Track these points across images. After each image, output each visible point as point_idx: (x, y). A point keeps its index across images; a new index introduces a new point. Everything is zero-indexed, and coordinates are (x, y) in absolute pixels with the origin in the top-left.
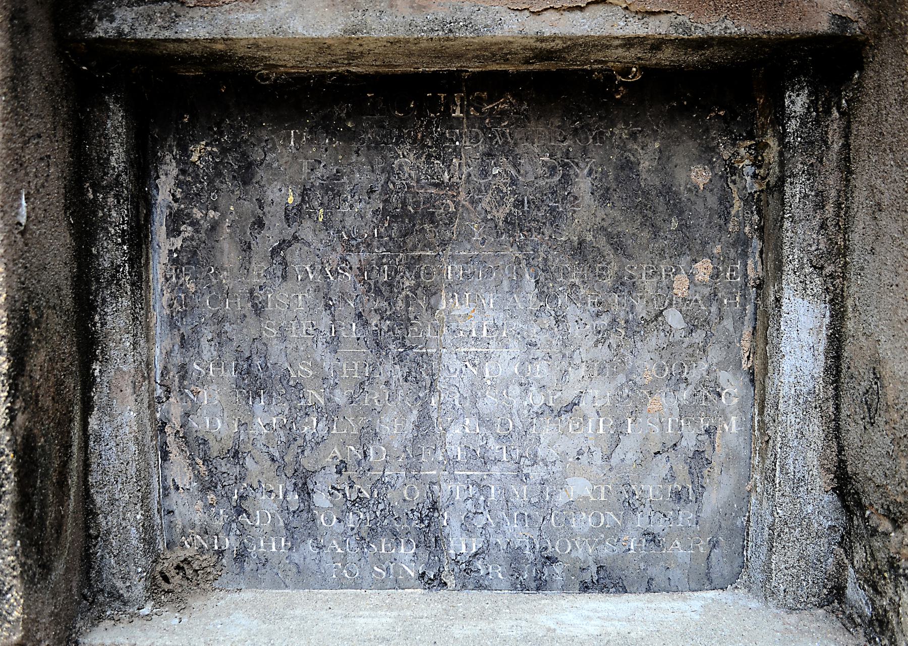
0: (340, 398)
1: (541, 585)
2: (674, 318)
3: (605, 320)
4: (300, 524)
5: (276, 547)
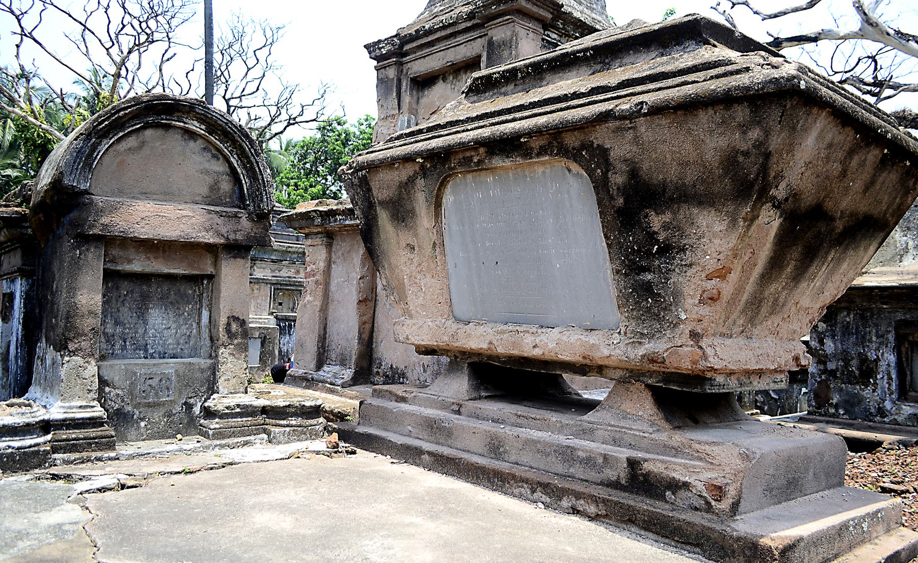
4: (124, 348)
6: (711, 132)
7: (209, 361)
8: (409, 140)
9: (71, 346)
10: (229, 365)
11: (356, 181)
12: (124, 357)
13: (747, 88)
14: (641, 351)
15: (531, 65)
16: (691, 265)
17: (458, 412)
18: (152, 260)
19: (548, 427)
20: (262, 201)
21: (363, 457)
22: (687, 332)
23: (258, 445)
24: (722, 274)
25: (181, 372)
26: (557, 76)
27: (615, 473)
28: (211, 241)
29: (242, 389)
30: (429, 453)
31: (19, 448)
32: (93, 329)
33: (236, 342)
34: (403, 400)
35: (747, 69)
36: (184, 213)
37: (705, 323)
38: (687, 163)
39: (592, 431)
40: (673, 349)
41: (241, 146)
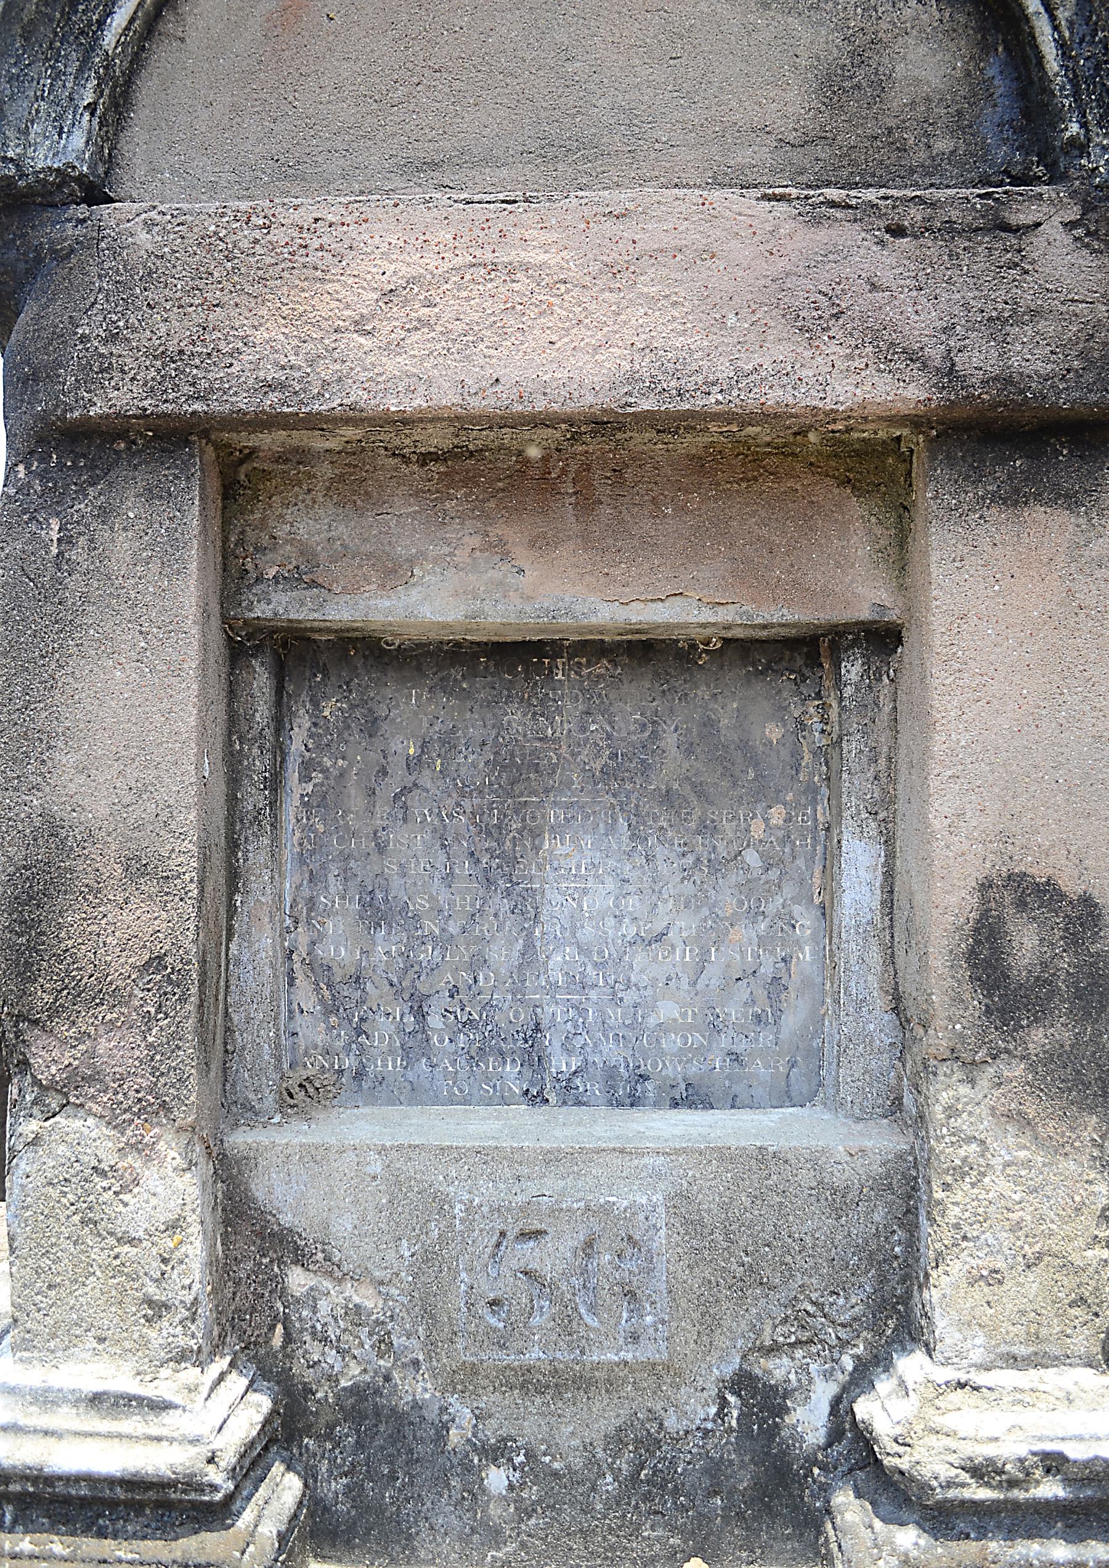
0: (453, 928)
1: (635, 1102)
2: (751, 858)
3: (690, 860)
4: (415, 1044)
5: (392, 1065)
7: (882, 1142)
9: (49, 1057)
10: (998, 1185)
12: (417, 1094)
18: (522, 555)
25: (709, 1203)
32: (157, 962)
33: (1038, 1038)
36: (651, 234)
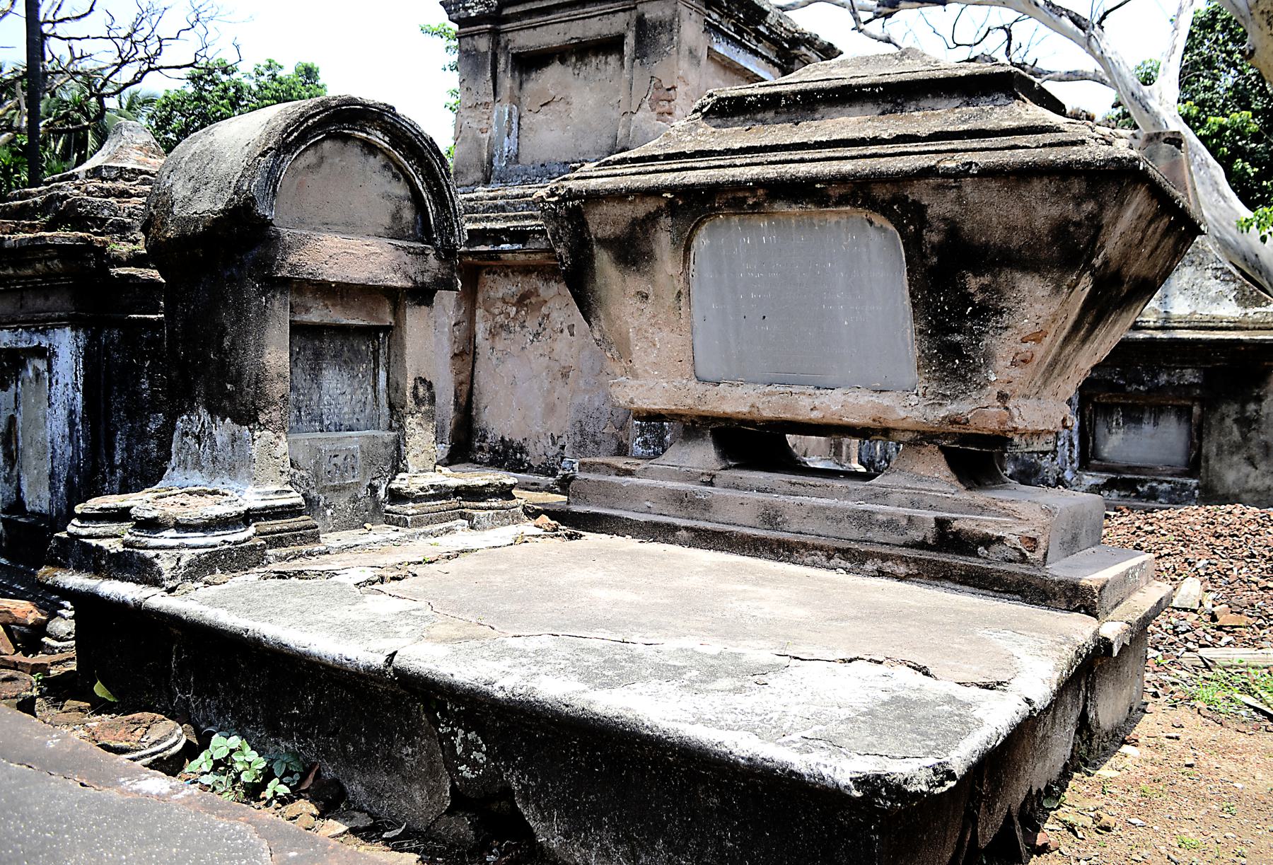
4: (299, 419)
6: (1044, 200)
8: (638, 167)
9: (262, 418)
11: (563, 212)
12: (299, 431)
13: (1088, 164)
14: (942, 413)
15: (800, 92)
16: (1006, 328)
17: (711, 484)
19: (832, 495)
20: (452, 234)
21: (592, 540)
22: (995, 393)
23: (460, 532)
24: (1037, 337)
26: (834, 109)
27: (922, 534)
28: (399, 284)
29: (431, 467)
30: (686, 528)
31: (236, 543)
34: (629, 473)
35: (1083, 142)
37: (1014, 385)
38: (1015, 228)
39: (885, 495)
40: (976, 409)
41: (430, 164)
